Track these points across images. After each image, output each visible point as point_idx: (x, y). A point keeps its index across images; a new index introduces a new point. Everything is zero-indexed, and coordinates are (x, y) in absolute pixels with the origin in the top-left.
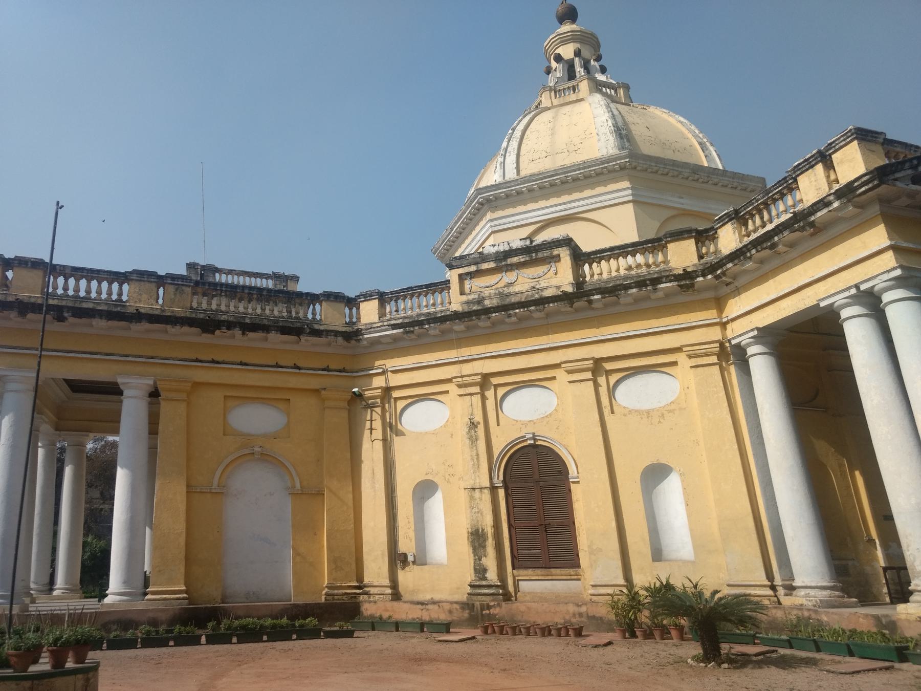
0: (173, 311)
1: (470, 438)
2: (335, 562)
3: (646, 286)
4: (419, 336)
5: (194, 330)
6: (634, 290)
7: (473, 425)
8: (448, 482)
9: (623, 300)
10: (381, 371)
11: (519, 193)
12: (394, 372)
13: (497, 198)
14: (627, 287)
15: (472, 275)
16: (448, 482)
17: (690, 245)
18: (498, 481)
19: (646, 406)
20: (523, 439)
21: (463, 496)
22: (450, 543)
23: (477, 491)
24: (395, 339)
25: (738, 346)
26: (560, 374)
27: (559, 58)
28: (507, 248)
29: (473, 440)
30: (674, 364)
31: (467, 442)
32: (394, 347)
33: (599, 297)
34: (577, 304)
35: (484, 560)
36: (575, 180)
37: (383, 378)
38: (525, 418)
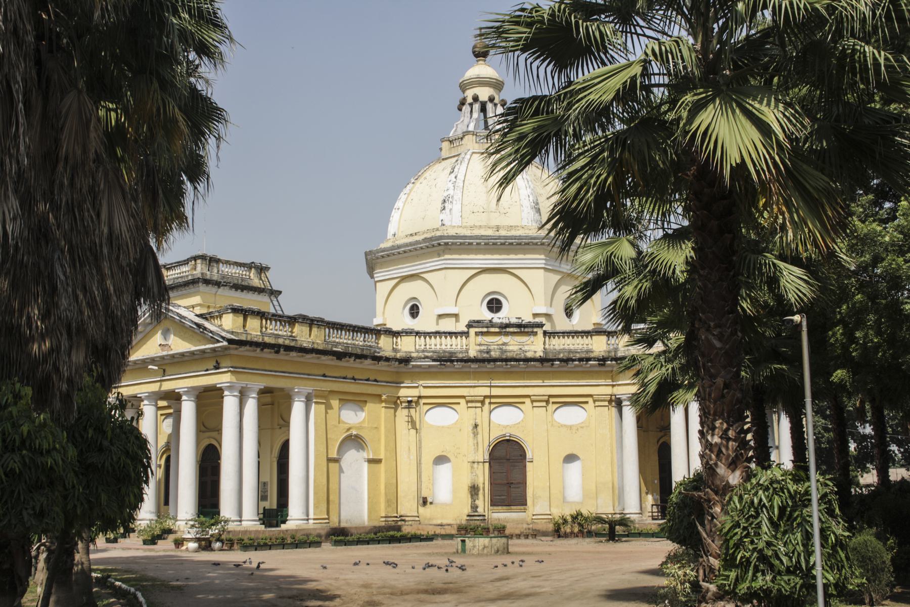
0: (317, 343)
1: (474, 433)
2: (388, 502)
3: (583, 361)
4: (449, 367)
5: (330, 357)
6: (577, 363)
7: (476, 426)
8: (456, 457)
9: (569, 366)
10: (417, 385)
11: (470, 244)
12: (425, 387)
13: (453, 244)
14: (573, 360)
15: (482, 333)
16: (456, 457)
17: (604, 338)
18: (487, 457)
19: (569, 423)
20: (504, 436)
21: (466, 466)
22: (455, 491)
23: (476, 464)
24: (430, 366)
25: (619, 398)
26: (527, 401)
27: (476, 99)
28: (508, 322)
29: (475, 434)
30: (587, 402)
31: (472, 435)
32: (427, 373)
33: (558, 363)
34: (546, 364)
35: (477, 502)
36: (511, 244)
38: (505, 423)
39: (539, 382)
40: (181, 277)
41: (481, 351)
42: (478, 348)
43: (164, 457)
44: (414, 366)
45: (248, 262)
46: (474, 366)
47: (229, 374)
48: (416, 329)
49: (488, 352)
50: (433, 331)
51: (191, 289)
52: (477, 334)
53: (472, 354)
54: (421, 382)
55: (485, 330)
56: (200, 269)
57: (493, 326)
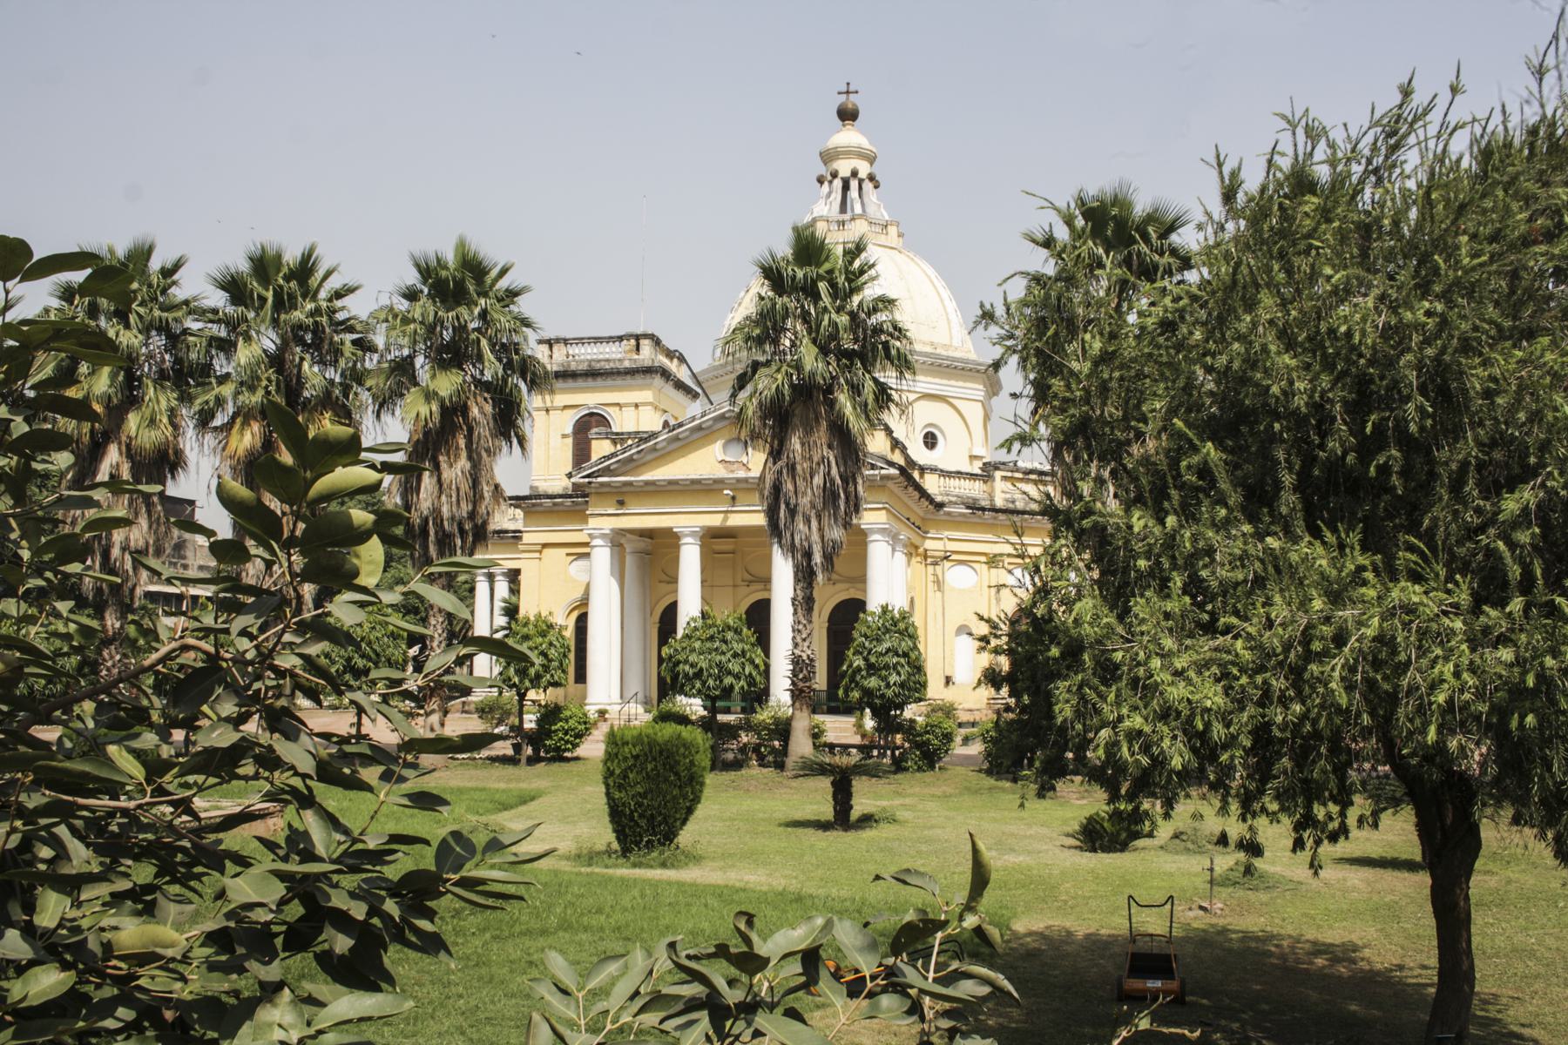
24: (963, 515)
27: (854, 174)
32: (956, 522)
37: (941, 542)
39: (990, 537)
40: (608, 360)
41: (1007, 500)
42: (1003, 495)
43: (575, 614)
44: (949, 514)
45: (672, 348)
46: (1002, 517)
47: (884, 512)
48: (941, 466)
49: (1013, 502)
50: (953, 469)
51: (639, 380)
52: (1005, 478)
53: (999, 502)
54: (947, 533)
55: (1009, 474)
56: (647, 354)
57: (1017, 471)
